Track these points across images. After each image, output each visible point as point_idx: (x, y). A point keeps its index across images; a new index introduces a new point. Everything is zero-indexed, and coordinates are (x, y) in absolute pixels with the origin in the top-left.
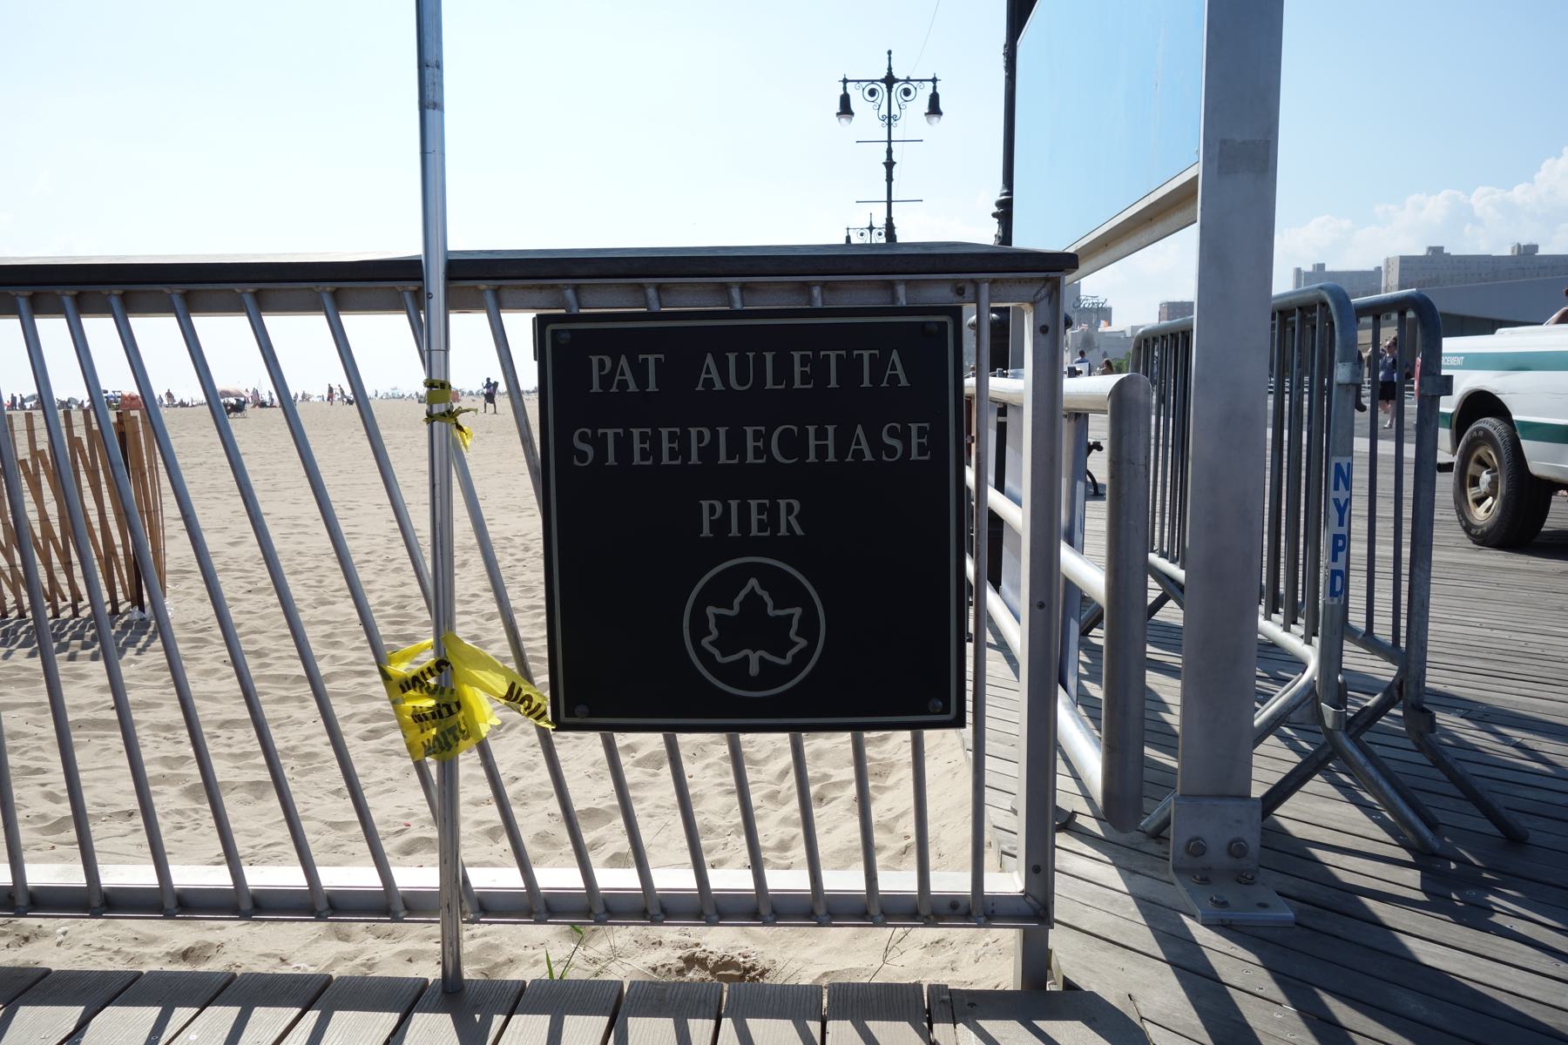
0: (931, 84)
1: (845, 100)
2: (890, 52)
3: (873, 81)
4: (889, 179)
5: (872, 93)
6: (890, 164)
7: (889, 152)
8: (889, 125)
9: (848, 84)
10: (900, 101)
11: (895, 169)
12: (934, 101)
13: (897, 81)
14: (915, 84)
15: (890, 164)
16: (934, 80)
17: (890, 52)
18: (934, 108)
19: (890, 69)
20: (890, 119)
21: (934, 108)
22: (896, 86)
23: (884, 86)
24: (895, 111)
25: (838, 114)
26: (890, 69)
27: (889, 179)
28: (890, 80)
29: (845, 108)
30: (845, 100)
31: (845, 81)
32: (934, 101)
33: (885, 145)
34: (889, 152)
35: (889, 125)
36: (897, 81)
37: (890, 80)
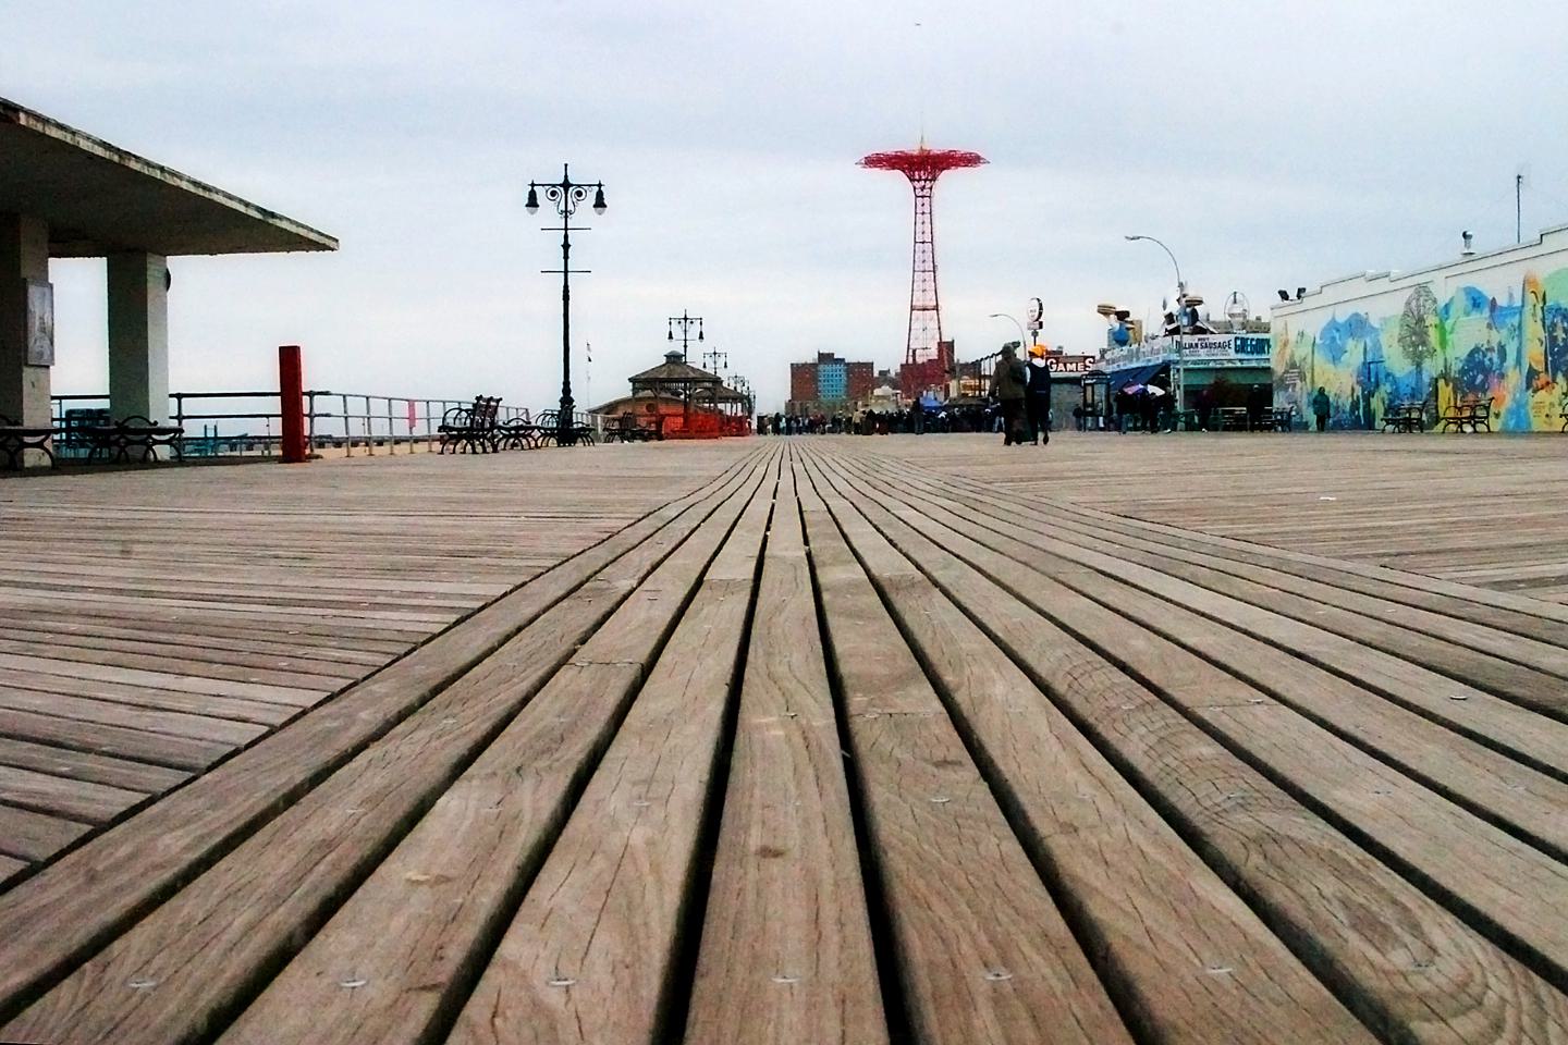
0: (597, 188)
1: (532, 195)
2: (566, 165)
3: (554, 186)
4: (566, 257)
5: (553, 193)
6: (566, 246)
7: (566, 237)
8: (566, 217)
9: (535, 188)
10: (575, 200)
11: (570, 250)
12: (600, 195)
13: (572, 185)
14: (586, 188)
15: (566, 246)
16: (600, 185)
17: (566, 165)
18: (600, 203)
19: (566, 176)
20: (566, 213)
21: (600, 203)
22: (571, 189)
23: (562, 189)
24: (570, 207)
25: (527, 206)
26: (566, 176)
27: (566, 257)
28: (566, 185)
29: (533, 202)
30: (532, 195)
31: (533, 185)
32: (600, 195)
33: (563, 232)
34: (566, 237)
35: (566, 217)
36: (572, 185)
37: (566, 185)
